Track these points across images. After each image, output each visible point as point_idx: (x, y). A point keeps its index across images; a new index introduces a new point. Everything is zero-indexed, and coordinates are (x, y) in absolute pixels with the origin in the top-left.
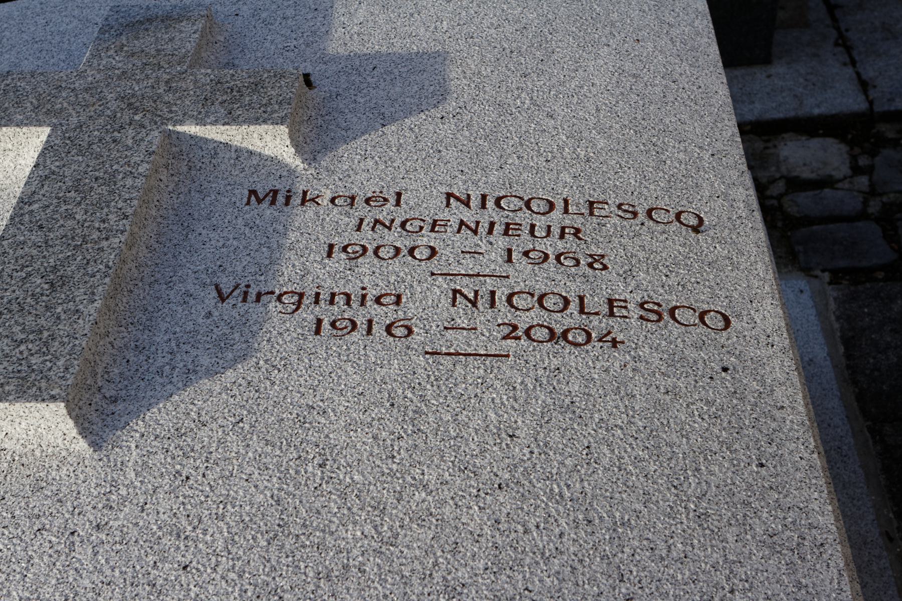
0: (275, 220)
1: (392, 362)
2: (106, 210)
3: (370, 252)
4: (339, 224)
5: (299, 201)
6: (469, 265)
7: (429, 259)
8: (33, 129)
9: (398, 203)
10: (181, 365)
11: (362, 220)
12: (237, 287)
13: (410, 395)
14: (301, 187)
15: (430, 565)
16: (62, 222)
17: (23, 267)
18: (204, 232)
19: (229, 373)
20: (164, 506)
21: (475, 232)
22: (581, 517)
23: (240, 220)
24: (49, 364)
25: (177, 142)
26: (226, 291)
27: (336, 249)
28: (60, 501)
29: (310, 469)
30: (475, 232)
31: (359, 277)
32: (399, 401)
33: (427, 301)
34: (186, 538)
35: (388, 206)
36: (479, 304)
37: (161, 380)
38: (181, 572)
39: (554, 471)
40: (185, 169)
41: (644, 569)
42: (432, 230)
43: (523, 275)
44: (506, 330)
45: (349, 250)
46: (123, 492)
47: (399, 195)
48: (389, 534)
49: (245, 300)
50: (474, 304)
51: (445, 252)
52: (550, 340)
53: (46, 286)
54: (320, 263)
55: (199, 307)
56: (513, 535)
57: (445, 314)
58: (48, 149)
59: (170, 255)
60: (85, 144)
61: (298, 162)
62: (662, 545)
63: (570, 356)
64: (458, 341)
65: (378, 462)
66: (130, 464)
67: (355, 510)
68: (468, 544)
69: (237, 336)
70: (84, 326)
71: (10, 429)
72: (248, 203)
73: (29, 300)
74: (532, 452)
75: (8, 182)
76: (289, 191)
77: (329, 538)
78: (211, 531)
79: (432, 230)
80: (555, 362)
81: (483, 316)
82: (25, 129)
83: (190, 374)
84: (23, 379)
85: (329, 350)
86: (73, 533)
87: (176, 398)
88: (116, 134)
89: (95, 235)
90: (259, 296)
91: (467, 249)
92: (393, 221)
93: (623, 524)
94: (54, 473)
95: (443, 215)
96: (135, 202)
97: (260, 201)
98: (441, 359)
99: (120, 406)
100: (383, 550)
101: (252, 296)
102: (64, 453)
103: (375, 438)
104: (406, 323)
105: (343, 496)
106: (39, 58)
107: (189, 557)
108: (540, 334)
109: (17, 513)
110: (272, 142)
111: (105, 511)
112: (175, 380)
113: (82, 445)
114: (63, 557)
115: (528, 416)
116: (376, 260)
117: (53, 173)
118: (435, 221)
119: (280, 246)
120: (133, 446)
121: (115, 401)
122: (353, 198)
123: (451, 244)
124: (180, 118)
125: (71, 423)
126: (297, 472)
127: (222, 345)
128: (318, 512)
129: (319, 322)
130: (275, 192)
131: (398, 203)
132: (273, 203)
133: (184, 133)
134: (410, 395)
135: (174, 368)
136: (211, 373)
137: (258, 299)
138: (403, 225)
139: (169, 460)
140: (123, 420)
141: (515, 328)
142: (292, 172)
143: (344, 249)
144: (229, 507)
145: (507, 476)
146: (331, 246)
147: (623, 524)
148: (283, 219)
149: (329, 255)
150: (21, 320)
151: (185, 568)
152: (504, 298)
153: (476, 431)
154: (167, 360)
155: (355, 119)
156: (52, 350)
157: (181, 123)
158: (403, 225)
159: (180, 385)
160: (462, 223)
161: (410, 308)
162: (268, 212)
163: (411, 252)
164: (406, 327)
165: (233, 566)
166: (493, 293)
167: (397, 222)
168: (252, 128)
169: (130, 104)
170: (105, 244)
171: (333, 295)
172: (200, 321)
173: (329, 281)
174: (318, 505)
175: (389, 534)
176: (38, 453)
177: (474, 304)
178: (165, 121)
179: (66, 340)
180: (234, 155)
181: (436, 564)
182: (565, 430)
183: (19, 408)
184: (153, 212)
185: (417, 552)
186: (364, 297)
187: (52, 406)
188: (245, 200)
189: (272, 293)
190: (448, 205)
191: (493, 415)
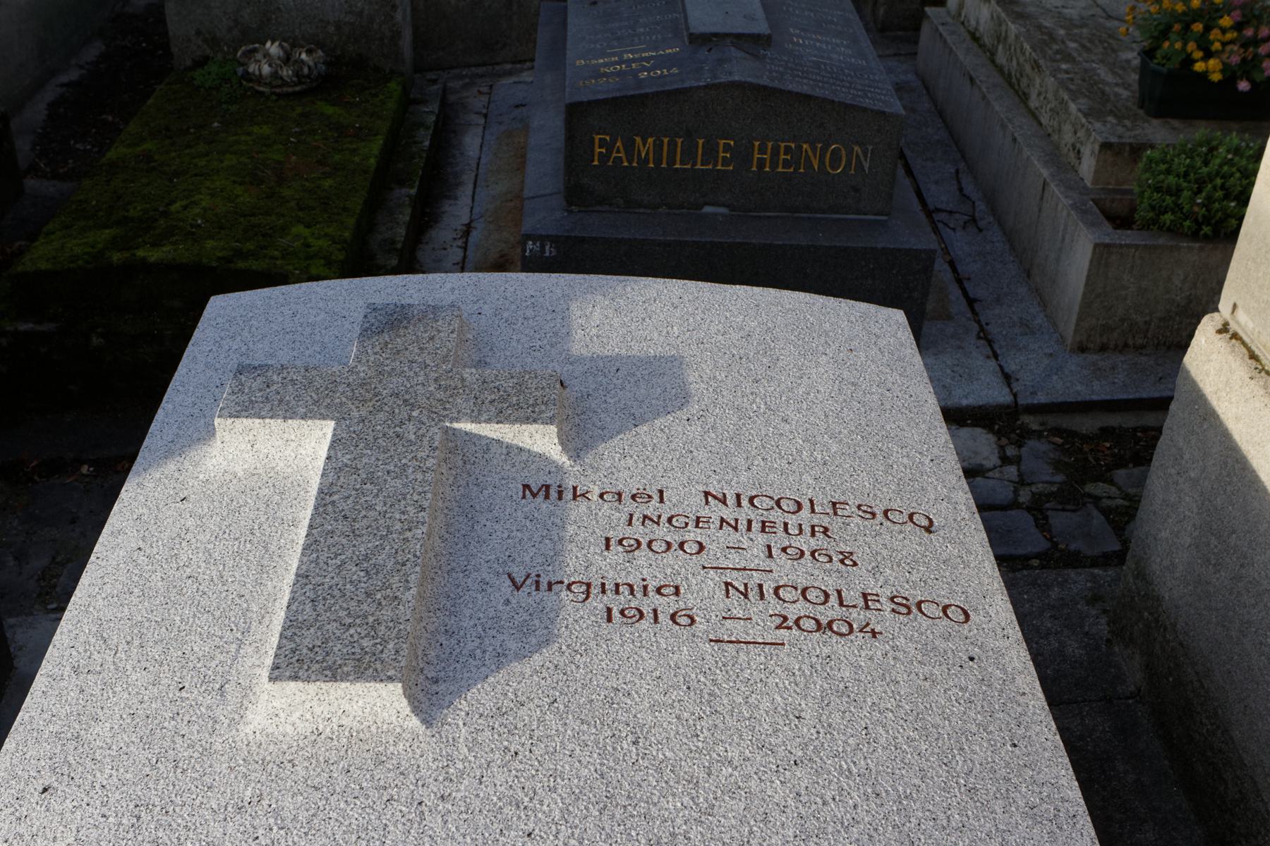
0: (552, 514)
1: (685, 650)
2: (403, 502)
3: (644, 546)
4: (611, 518)
5: (570, 496)
6: (735, 559)
7: (698, 553)
8: (317, 422)
9: (662, 501)
10: (491, 649)
11: (631, 515)
12: (528, 576)
13: (702, 679)
14: (570, 483)
15: (746, 833)
16: (364, 513)
17: (336, 556)
18: (488, 524)
19: (536, 656)
20: (499, 779)
21: (736, 529)
22: (869, 790)
23: (519, 513)
24: (380, 648)
25: (453, 438)
26: (519, 580)
27: (612, 542)
28: (402, 773)
29: (625, 746)
30: (736, 529)
31: (638, 568)
32: (694, 684)
33: (703, 592)
34: (525, 808)
35: (653, 502)
36: (750, 595)
37: (475, 663)
38: (526, 839)
39: (840, 749)
40: (461, 463)
41: (930, 837)
42: (697, 526)
43: (802, 573)
44: (778, 621)
45: (624, 543)
46: (460, 765)
47: (661, 492)
48: (706, 805)
49: (537, 589)
50: (746, 596)
51: (711, 547)
52: (817, 631)
53: (362, 574)
54: (601, 555)
55: (497, 595)
56: (814, 807)
57: (722, 605)
58: (336, 442)
59: (461, 545)
60: (370, 438)
61: (565, 459)
62: (942, 816)
63: (838, 646)
64: (737, 630)
65: (685, 740)
66: (461, 740)
67: (671, 783)
68: (776, 814)
69: (537, 622)
70: (404, 611)
71: (347, 707)
72: (524, 497)
73: (348, 586)
74: (818, 733)
75: (289, 470)
76: (560, 486)
77: (653, 809)
78: (546, 802)
79: (697, 526)
80: (826, 651)
81: (755, 607)
82: (310, 422)
83: (501, 659)
84: (359, 660)
85: (621, 636)
86: (420, 804)
87: (491, 679)
88: (397, 429)
89: (398, 526)
90: (550, 585)
91: (731, 545)
92: (659, 517)
93: (906, 797)
94: (392, 748)
95: (704, 512)
96: (429, 496)
97: (534, 495)
98: (725, 646)
99: (442, 687)
100: (703, 819)
101: (544, 586)
102: (398, 730)
103: (678, 718)
104: (688, 612)
105: (659, 770)
106: (293, 349)
107: (531, 825)
108: (809, 624)
109: (364, 784)
110: (541, 440)
111: (446, 783)
112: (487, 662)
113: (415, 722)
114: (416, 825)
115: (809, 699)
116: (651, 554)
117: (346, 466)
118: (698, 518)
119: (561, 539)
120: (461, 723)
121: (437, 682)
122: (620, 494)
123: (717, 539)
124: (455, 415)
125: (405, 702)
126: (614, 749)
127: (525, 631)
128: (639, 785)
129: (609, 610)
130: (548, 487)
131: (662, 501)
132: (547, 497)
133: (460, 430)
134: (702, 679)
135: (484, 652)
136: (520, 656)
137: (550, 589)
138: (670, 520)
139: (496, 736)
140: (447, 699)
141: (785, 619)
142: (559, 468)
143: (620, 542)
144: (559, 780)
145: (800, 753)
146: (608, 540)
147: (906, 797)
148: (558, 512)
149: (608, 547)
150: (345, 605)
151: (529, 835)
152: (771, 591)
153: (767, 713)
154: (477, 644)
155: (609, 419)
156: (380, 634)
157: (457, 420)
158: (670, 520)
159: (493, 667)
160: (722, 520)
161: (689, 599)
162: (544, 506)
163: (681, 545)
164: (689, 616)
165: (573, 834)
166: (760, 586)
167: (664, 518)
168: (524, 426)
169: (405, 401)
170: (408, 534)
171: (617, 585)
172: (500, 607)
173: (611, 572)
174: (638, 778)
175: (706, 805)
176: (373, 729)
177: (746, 596)
178: (442, 418)
179: (391, 624)
180: (505, 451)
181: (751, 832)
182: (844, 712)
183: (359, 687)
184: (440, 504)
185: (733, 822)
186: (645, 587)
187: (391, 686)
188: (521, 494)
189: (562, 582)
190: (707, 502)
191: (779, 699)
